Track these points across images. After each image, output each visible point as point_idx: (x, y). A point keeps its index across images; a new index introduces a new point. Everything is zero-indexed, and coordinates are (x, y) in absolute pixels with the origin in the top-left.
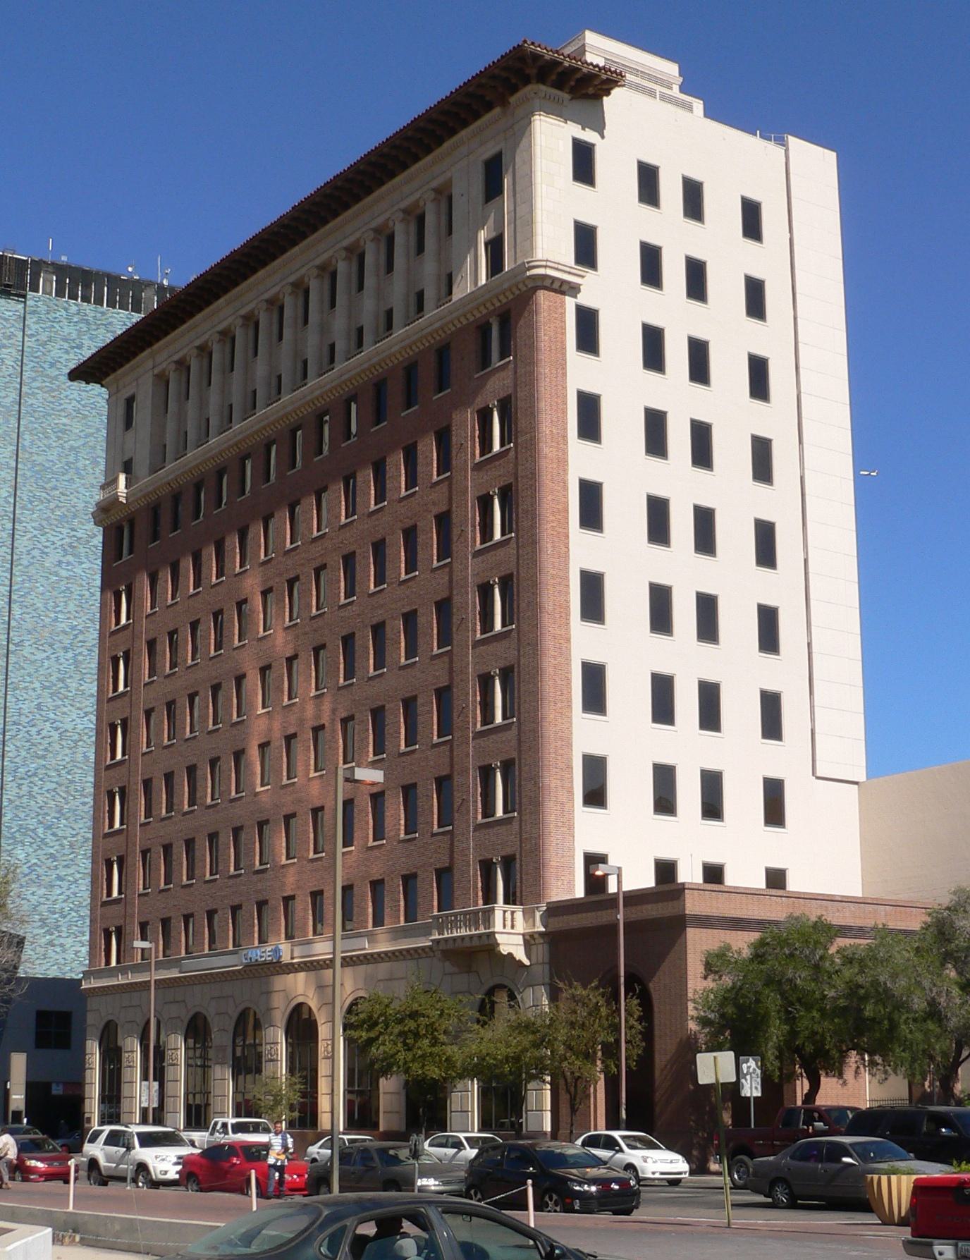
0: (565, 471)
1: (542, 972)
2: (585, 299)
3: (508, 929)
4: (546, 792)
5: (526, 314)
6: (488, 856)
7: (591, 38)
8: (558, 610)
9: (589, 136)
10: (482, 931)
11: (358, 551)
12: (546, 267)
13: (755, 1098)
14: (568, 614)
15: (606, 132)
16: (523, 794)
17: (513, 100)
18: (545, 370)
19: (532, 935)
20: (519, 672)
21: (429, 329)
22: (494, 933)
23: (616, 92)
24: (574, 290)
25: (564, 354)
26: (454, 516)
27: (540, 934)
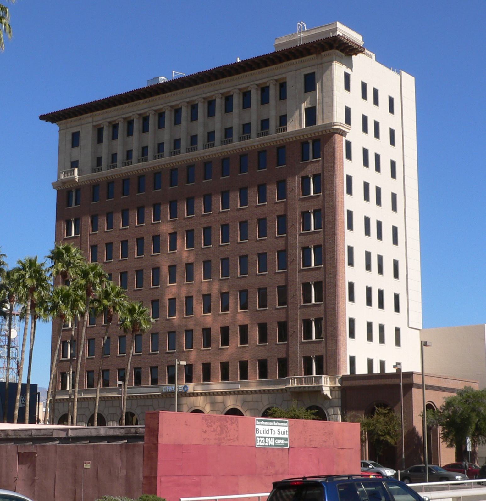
0: (344, 208)
1: (338, 402)
2: (348, 137)
3: (325, 385)
4: (339, 332)
5: (329, 142)
6: (308, 355)
7: (339, 25)
8: (342, 261)
9: (348, 71)
10: (314, 385)
11: (231, 224)
12: (340, 125)
13: (470, 452)
14: (345, 263)
15: (353, 69)
16: (328, 332)
17: (323, 53)
18: (338, 166)
19: (334, 388)
20: (325, 285)
21: (276, 139)
22: (322, 386)
23: (360, 55)
24: (343, 134)
25: (343, 160)
26: (288, 217)
27: (338, 387)
